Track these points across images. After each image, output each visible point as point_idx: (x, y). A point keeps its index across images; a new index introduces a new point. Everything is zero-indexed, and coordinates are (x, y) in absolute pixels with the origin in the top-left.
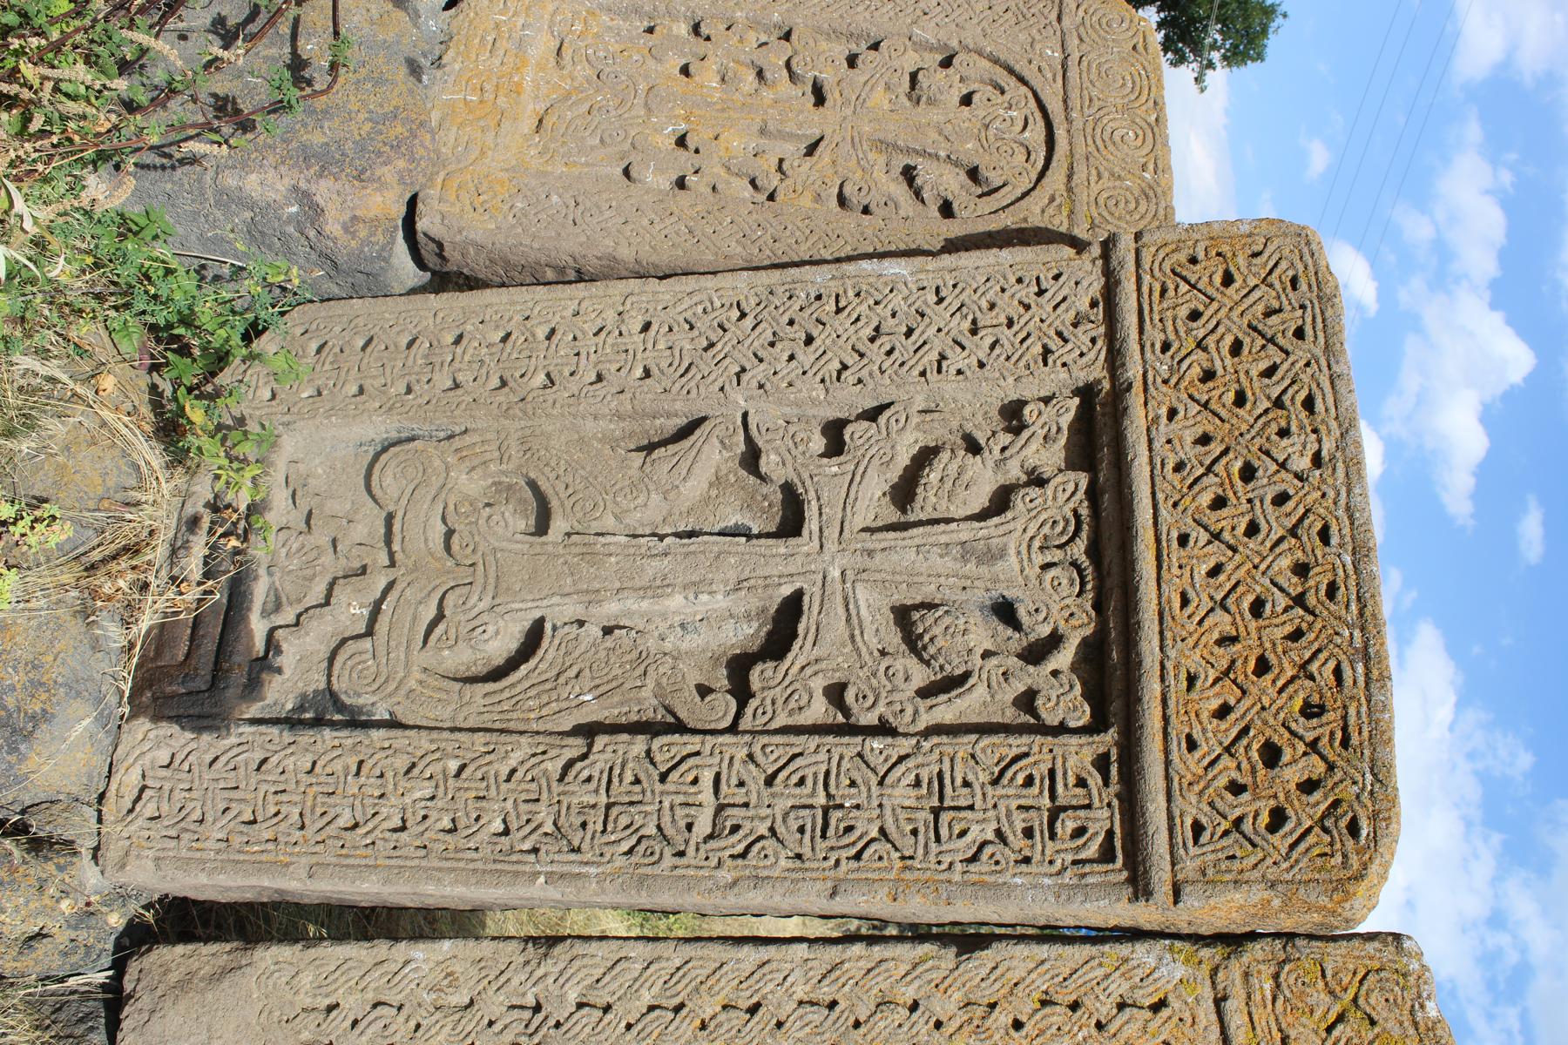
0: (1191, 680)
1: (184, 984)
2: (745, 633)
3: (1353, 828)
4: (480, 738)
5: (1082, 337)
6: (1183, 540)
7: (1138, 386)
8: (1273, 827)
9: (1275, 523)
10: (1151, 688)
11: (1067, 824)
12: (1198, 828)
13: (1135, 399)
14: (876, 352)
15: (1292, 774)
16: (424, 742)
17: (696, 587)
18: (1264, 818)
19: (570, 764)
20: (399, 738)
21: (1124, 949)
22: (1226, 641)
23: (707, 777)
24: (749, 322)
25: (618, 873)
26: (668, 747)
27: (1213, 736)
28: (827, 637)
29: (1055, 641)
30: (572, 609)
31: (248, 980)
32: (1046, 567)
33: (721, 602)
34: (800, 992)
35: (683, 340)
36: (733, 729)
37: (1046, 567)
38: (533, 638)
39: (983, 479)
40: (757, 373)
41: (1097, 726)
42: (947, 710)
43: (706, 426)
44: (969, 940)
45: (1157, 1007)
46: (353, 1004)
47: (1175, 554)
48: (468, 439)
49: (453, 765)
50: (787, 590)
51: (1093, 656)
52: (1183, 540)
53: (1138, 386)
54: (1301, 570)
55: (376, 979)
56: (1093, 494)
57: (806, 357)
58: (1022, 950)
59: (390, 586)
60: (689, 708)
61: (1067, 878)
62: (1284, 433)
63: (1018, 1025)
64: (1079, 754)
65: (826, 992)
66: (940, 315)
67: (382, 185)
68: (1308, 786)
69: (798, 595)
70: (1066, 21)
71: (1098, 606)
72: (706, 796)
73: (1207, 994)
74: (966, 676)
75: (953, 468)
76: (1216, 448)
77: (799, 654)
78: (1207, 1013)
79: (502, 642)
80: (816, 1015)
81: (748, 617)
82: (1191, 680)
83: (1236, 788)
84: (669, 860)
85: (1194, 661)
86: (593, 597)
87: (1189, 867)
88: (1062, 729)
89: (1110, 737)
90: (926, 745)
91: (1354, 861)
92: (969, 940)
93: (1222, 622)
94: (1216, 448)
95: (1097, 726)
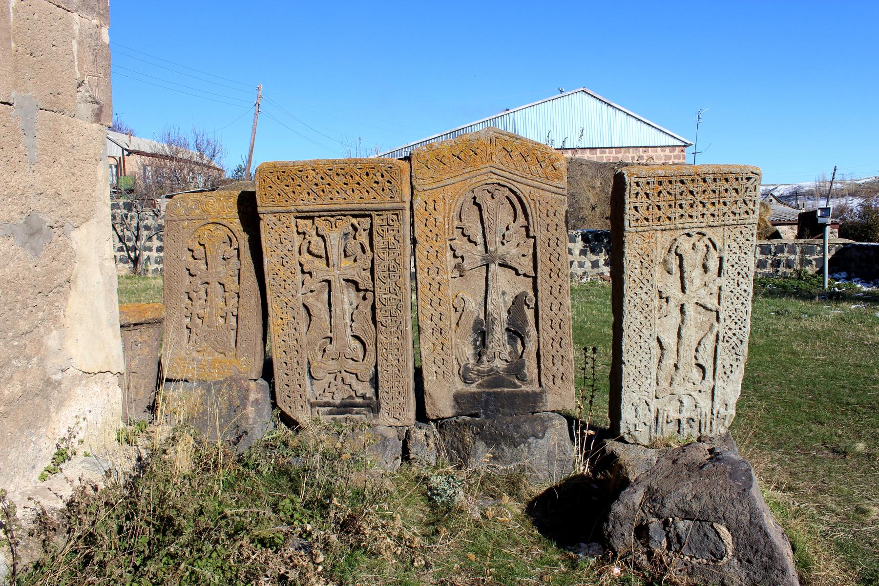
0: (361, 198)
1: (433, 404)
2: (352, 291)
3: (391, 168)
4: (378, 345)
5: (283, 219)
6: (331, 199)
7: (296, 207)
8: (391, 183)
9: (328, 179)
10: (363, 206)
11: (391, 223)
12: (391, 197)
13: (299, 208)
14: (287, 265)
15: (380, 178)
16: (379, 357)
17: (342, 302)
18: (389, 184)
19: (382, 325)
20: (379, 363)
21: (415, 209)
22: (353, 191)
23: (384, 296)
24: (280, 295)
25: (405, 313)
26: (378, 305)
27: (373, 194)
28: (353, 273)
29: (353, 225)
30: (349, 329)
31: (431, 390)
32: (336, 227)
33: (345, 297)
34: (426, 275)
35: (285, 310)
36: (374, 292)
37: (336, 227)
38: (356, 337)
39: (316, 240)
40: (293, 292)
41: (370, 216)
42: (368, 248)
43: (305, 303)
44: (414, 241)
45: (426, 203)
46: (435, 368)
47: (335, 201)
48: (310, 358)
49: (384, 350)
50: (343, 282)
51: (354, 216)
52: (331, 199)
53: (296, 207)
54: (338, 175)
55: (429, 363)
56: (320, 217)
57: (288, 281)
58: (416, 231)
59: (346, 371)
60: (369, 302)
61: (402, 223)
62: (307, 177)
63: (431, 231)
64: (377, 220)
65: (426, 270)
66: (278, 252)
67: (249, 385)
68: (382, 176)
69: (344, 280)
70: (176, 219)
71: (345, 215)
72: (388, 296)
73: (423, 193)
74: (361, 244)
75: (314, 248)
76: (310, 191)
77: (357, 279)
78: (427, 193)
79: (357, 344)
80: (431, 272)
81: (348, 291)
82: (361, 198)
83: (383, 190)
84: (402, 303)
85: (357, 198)
86: (345, 325)
87: (398, 199)
88: (371, 225)
89: (373, 214)
90: (375, 251)
91: (397, 168)
92: (414, 241)
93: (349, 192)
94: (310, 191)
95: (370, 216)
